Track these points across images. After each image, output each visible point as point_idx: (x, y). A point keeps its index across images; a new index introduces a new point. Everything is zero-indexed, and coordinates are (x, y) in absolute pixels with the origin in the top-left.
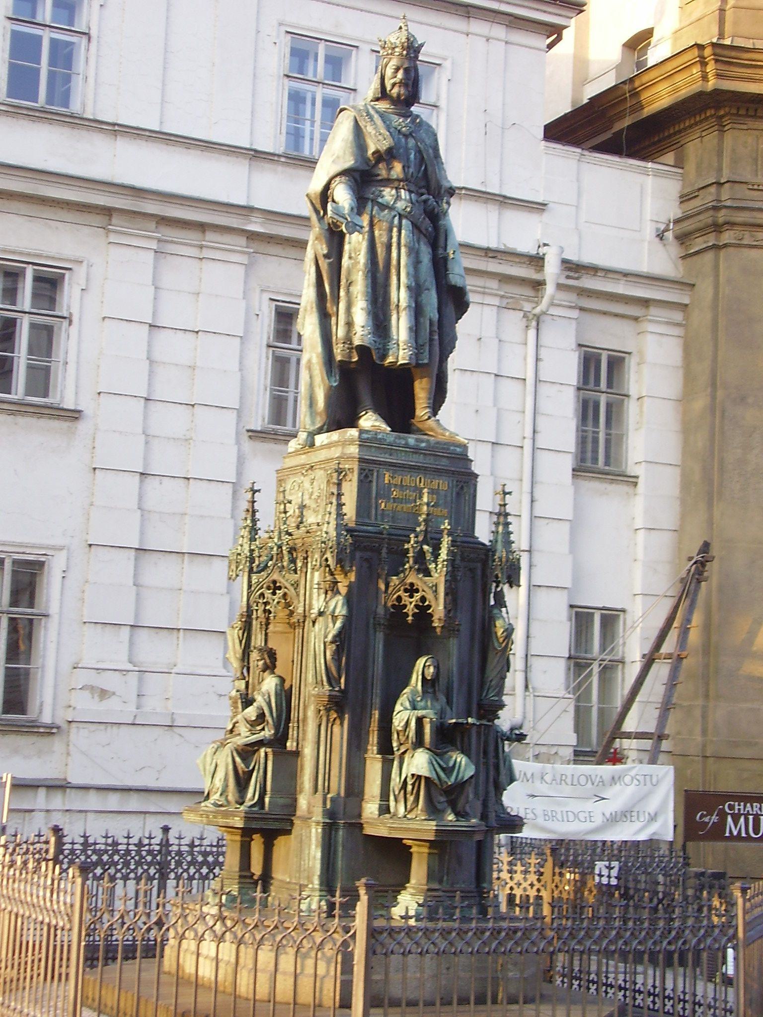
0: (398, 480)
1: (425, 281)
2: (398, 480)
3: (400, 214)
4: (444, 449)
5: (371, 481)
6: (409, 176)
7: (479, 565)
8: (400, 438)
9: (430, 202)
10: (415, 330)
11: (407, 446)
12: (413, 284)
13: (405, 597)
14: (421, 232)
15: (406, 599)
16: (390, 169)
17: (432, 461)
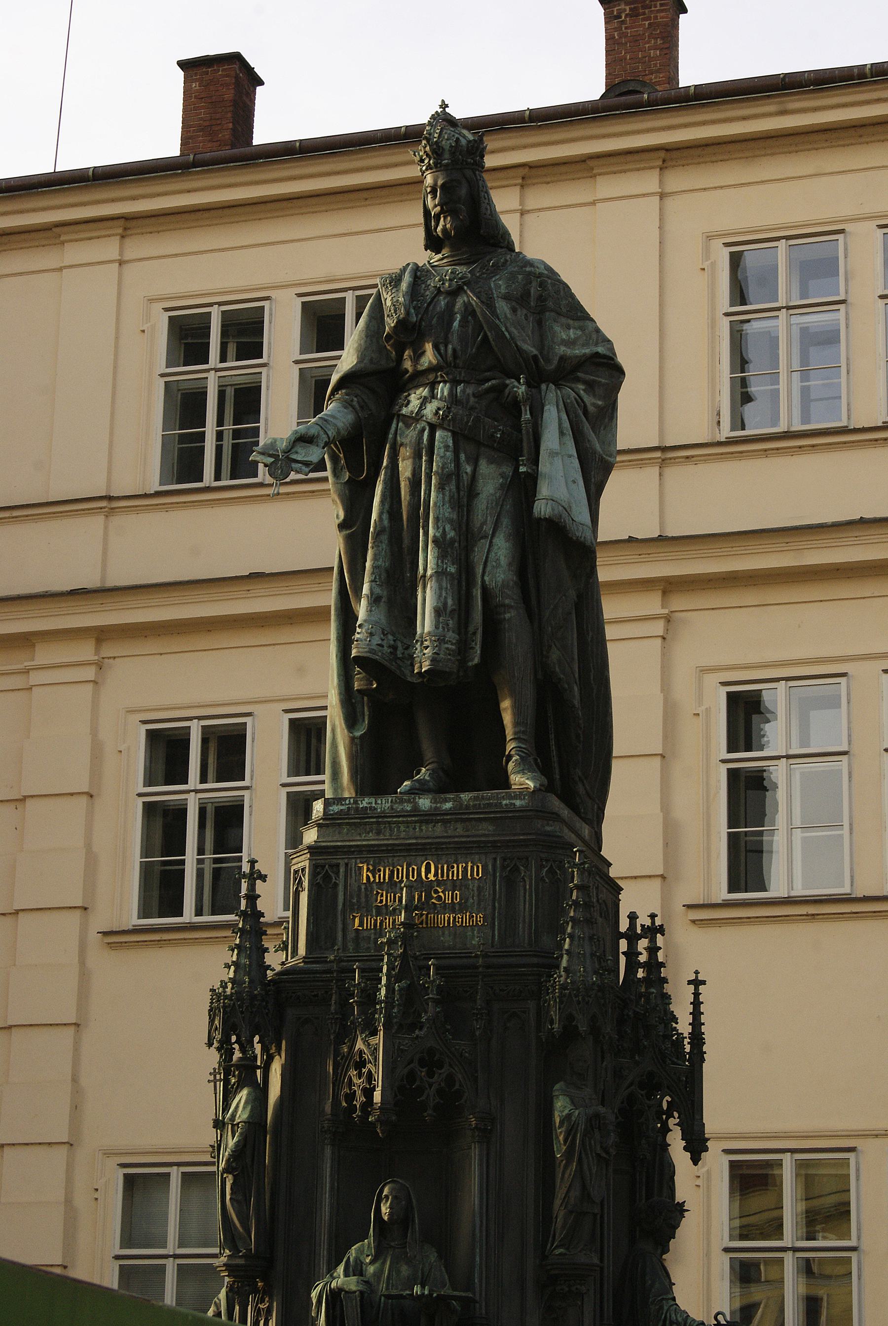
0: (384, 874)
1: (484, 523)
2: (384, 874)
3: (430, 424)
4: (490, 805)
5: (336, 885)
6: (450, 358)
7: (531, 1005)
8: (402, 801)
9: (507, 391)
10: (456, 612)
11: (416, 810)
12: (451, 534)
13: (353, 1073)
14: (479, 444)
15: (355, 1080)
16: (418, 355)
17: (460, 831)
